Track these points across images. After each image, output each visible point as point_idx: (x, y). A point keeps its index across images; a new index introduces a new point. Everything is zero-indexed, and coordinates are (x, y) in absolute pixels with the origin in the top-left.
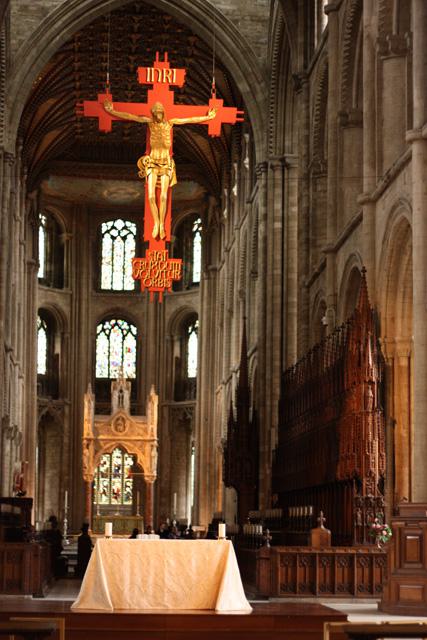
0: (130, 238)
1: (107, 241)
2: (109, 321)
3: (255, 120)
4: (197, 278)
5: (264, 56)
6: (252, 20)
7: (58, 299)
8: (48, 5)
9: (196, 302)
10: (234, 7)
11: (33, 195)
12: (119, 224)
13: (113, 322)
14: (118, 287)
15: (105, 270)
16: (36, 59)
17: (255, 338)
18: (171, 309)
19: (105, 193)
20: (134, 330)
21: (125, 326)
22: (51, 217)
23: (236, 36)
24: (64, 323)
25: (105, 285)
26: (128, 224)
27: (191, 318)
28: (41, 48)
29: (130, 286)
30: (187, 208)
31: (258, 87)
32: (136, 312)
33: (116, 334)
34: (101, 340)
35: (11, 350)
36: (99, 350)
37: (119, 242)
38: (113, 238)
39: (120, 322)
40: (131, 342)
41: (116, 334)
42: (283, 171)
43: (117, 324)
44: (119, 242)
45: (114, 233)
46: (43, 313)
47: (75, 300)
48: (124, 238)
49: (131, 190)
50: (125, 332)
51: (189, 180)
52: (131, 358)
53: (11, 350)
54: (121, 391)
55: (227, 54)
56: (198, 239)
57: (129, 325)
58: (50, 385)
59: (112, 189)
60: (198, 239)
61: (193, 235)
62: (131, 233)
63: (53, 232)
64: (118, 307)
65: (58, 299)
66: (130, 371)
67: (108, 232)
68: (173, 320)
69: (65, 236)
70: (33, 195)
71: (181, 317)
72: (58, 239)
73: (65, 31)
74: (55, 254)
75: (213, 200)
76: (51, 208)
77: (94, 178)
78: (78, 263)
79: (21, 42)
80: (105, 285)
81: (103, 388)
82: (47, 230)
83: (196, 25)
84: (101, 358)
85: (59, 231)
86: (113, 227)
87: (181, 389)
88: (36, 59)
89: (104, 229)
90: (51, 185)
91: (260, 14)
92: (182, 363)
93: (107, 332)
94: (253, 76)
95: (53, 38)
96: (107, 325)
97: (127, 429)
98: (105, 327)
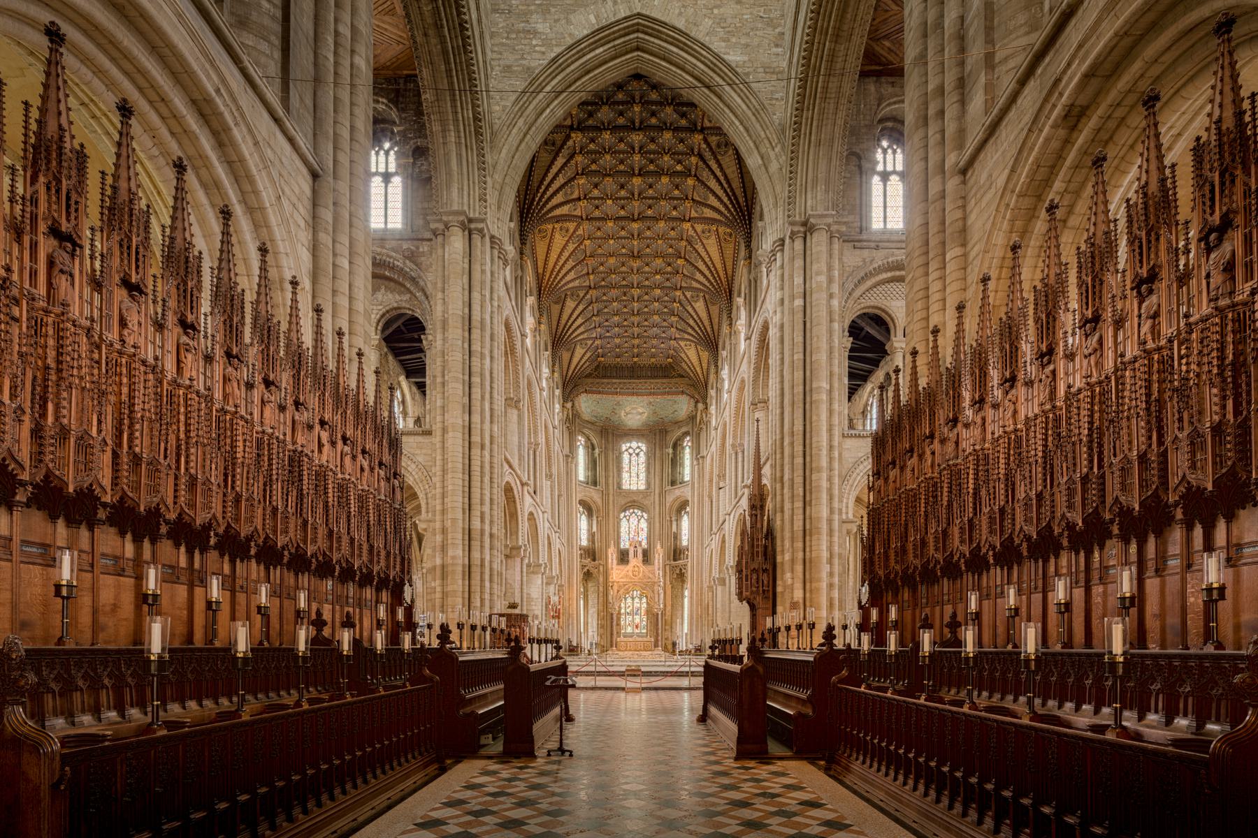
0: (642, 454)
1: (626, 456)
3: (767, 197)
4: (687, 478)
6: (766, 73)
7: (594, 495)
8: (534, 64)
10: (746, 58)
11: (569, 405)
12: (634, 444)
14: (634, 488)
15: (625, 475)
16: (525, 136)
18: (670, 499)
19: (623, 414)
20: (645, 515)
22: (588, 439)
24: (598, 511)
25: (625, 486)
28: (530, 120)
29: (642, 487)
31: (772, 154)
32: (646, 502)
33: (634, 520)
34: (624, 523)
35: (527, 484)
36: (622, 530)
37: (634, 458)
40: (644, 525)
41: (634, 520)
42: (805, 239)
44: (634, 458)
46: (582, 503)
47: (605, 495)
49: (640, 410)
51: (683, 393)
53: (527, 484)
55: (737, 123)
56: (687, 450)
59: (628, 409)
60: (687, 450)
61: (683, 448)
63: (591, 447)
64: (633, 502)
68: (671, 506)
69: (597, 451)
70: (569, 405)
71: (677, 504)
72: (593, 454)
73: (556, 102)
74: (592, 464)
75: (700, 406)
76: (586, 431)
77: (612, 394)
78: (606, 469)
79: (505, 107)
80: (625, 486)
82: (586, 447)
84: (624, 535)
85: (593, 449)
88: (525, 136)
89: (624, 448)
91: (775, 65)
94: (766, 141)
95: (541, 114)
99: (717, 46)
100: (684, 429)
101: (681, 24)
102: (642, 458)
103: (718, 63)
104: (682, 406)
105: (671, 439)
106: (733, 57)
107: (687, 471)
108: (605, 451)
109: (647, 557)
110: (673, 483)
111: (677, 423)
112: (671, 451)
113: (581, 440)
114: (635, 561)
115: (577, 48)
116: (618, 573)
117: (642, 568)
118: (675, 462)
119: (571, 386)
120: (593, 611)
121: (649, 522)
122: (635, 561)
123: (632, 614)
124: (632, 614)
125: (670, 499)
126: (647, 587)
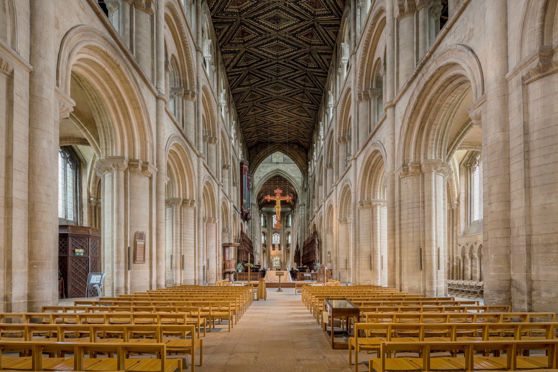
5: (300, 184)
9: (290, 230)
17: (299, 236)
23: (295, 181)
27: (289, 233)
33: (276, 236)
34: (273, 237)
40: (279, 237)
41: (276, 236)
47: (268, 230)
52: (279, 240)
58: (265, 245)
63: (265, 217)
64: (276, 231)
65: (265, 230)
66: (279, 242)
81: (274, 246)
83: (288, 179)
84: (273, 240)
87: (288, 245)
90: (264, 209)
92: (287, 241)
99: (290, 173)
101: (284, 170)
103: (290, 176)
104: (289, 209)
105: (286, 215)
106: (293, 175)
107: (290, 223)
108: (269, 218)
109: (280, 249)
110: (287, 227)
111: (288, 212)
113: (262, 215)
114: (277, 250)
115: (268, 174)
116: (272, 253)
117: (278, 251)
118: (287, 221)
119: (260, 207)
120: (265, 261)
121: (280, 236)
122: (277, 250)
123: (276, 261)
124: (276, 261)
125: (286, 231)
126: (279, 256)
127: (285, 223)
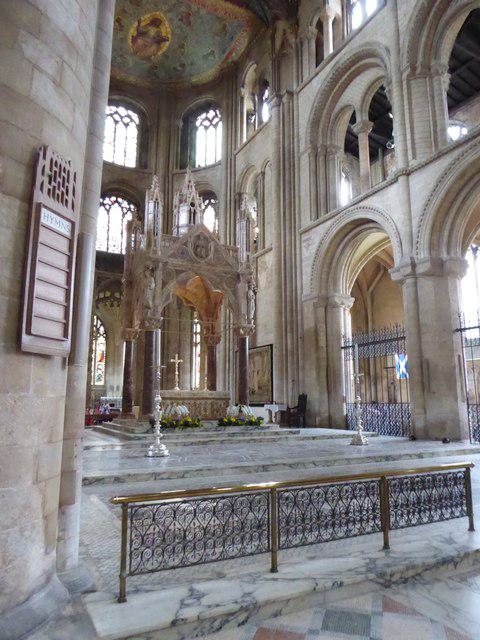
2: (110, 197)
12: (122, 110)
13: (113, 199)
21: (125, 204)
26: (130, 113)
30: (199, 93)
33: (116, 209)
38: (116, 122)
39: (120, 200)
43: (116, 201)
45: (117, 117)
48: (126, 125)
49: (166, 29)
50: (125, 211)
54: (192, 205)
57: (129, 204)
61: (196, 128)
62: (132, 120)
67: (111, 115)
86: (116, 113)
93: (107, 207)
96: (107, 201)
97: (211, 256)
98: (105, 202)
100: (202, 100)
102: (133, 132)
112: (181, 124)
127: (176, 148)
